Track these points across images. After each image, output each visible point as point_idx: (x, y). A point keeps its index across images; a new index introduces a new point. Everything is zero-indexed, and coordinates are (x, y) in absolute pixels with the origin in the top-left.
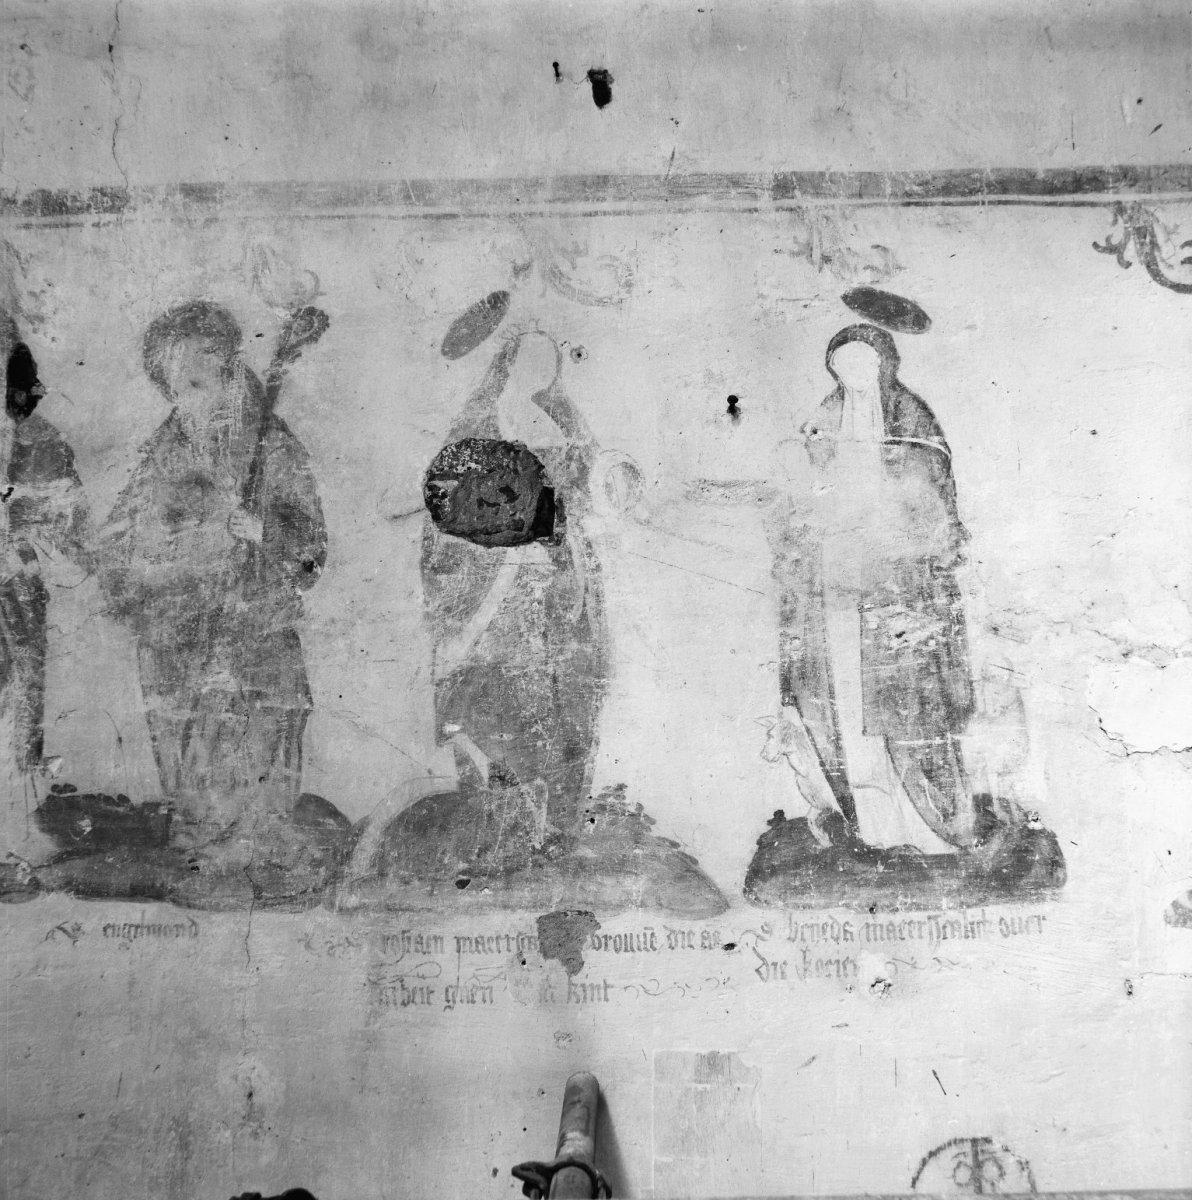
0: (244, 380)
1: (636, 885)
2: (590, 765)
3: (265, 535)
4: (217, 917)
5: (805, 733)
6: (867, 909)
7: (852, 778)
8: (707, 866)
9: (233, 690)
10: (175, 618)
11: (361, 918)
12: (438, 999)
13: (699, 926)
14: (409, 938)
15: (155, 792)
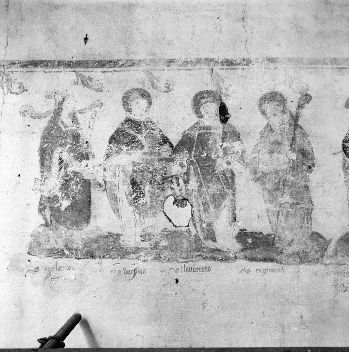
0: (288, 114)
3: (297, 158)
4: (289, 267)
9: (291, 202)
10: (273, 181)
11: (331, 267)
14: (345, 272)
15: (270, 231)
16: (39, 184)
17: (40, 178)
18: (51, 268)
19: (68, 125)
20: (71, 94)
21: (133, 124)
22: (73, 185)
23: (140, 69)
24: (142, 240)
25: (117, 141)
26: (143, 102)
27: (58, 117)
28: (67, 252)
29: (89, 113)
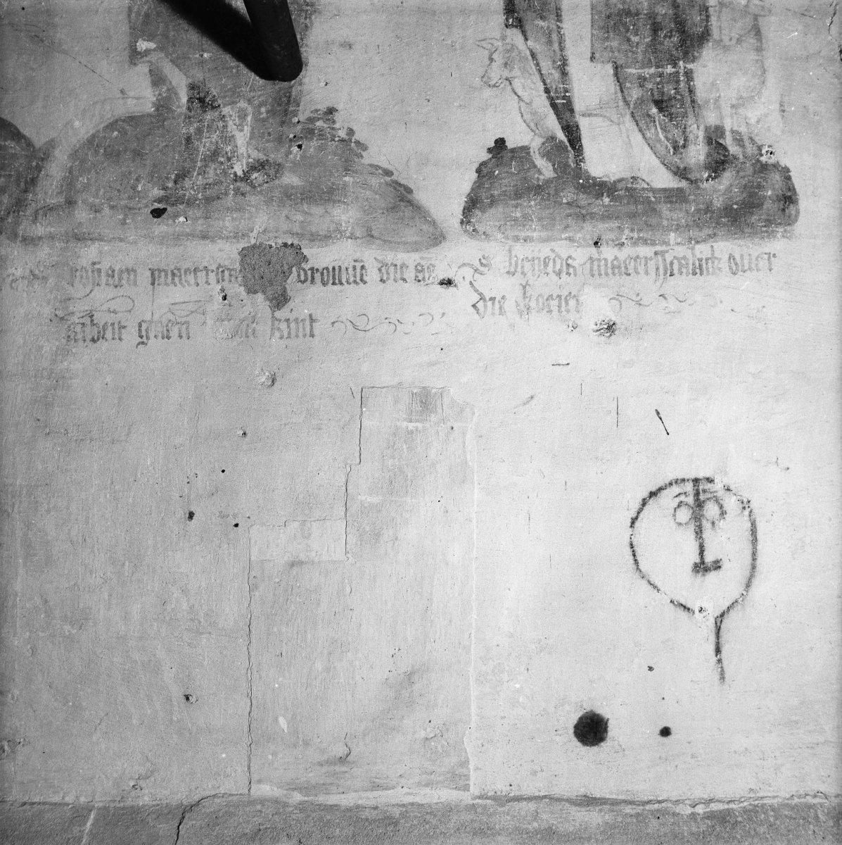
1: (346, 215)
2: (299, 88)
5: (530, 58)
6: (591, 243)
7: (578, 106)
8: (421, 197)
12: (131, 336)
13: (411, 259)
14: (99, 271)
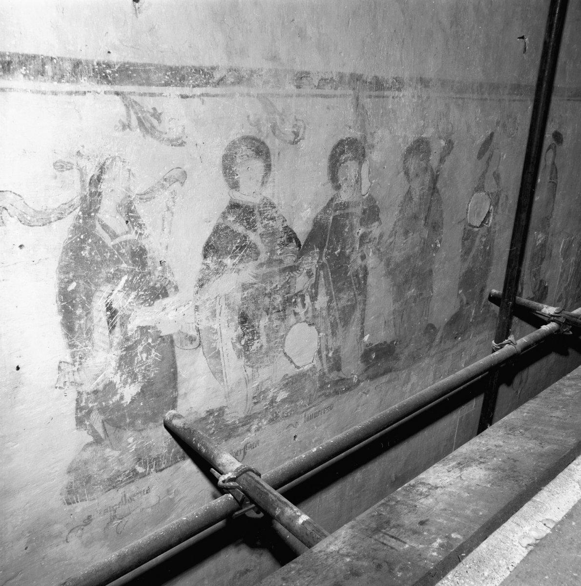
16: (68, 373)
17: (69, 360)
18: (115, 505)
19: (118, 232)
20: (117, 154)
21: (241, 214)
22: (141, 353)
23: (253, 91)
24: (255, 403)
25: (217, 251)
26: (258, 165)
27: (93, 214)
28: (140, 470)
29: (163, 198)
